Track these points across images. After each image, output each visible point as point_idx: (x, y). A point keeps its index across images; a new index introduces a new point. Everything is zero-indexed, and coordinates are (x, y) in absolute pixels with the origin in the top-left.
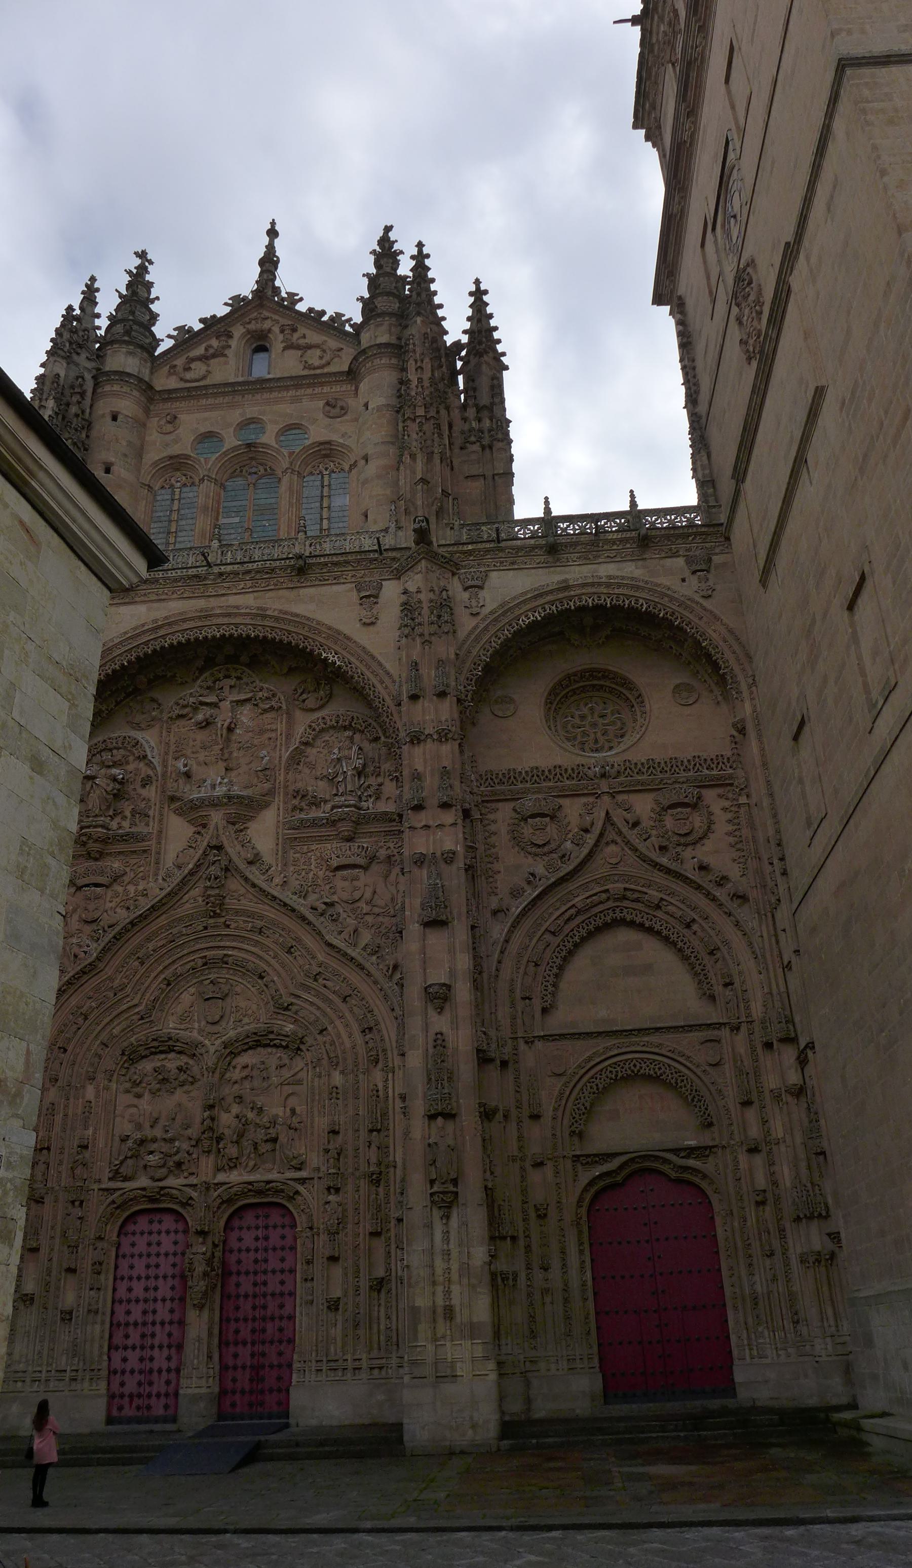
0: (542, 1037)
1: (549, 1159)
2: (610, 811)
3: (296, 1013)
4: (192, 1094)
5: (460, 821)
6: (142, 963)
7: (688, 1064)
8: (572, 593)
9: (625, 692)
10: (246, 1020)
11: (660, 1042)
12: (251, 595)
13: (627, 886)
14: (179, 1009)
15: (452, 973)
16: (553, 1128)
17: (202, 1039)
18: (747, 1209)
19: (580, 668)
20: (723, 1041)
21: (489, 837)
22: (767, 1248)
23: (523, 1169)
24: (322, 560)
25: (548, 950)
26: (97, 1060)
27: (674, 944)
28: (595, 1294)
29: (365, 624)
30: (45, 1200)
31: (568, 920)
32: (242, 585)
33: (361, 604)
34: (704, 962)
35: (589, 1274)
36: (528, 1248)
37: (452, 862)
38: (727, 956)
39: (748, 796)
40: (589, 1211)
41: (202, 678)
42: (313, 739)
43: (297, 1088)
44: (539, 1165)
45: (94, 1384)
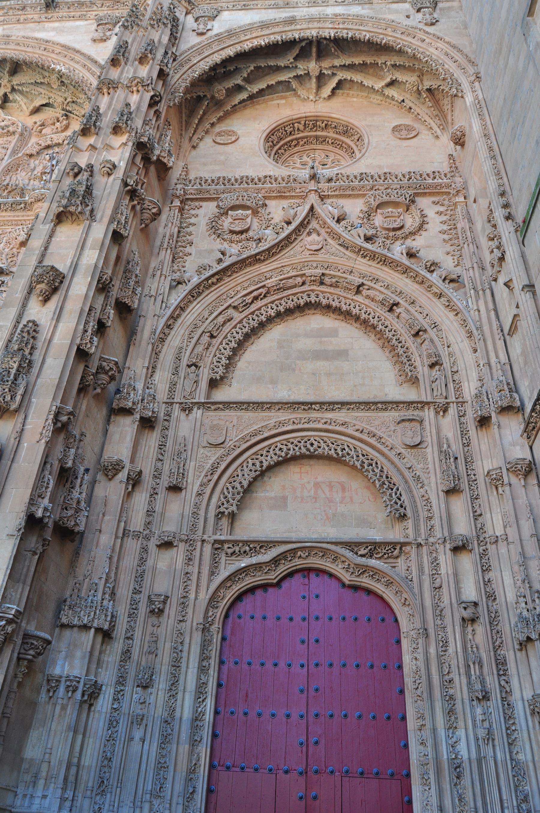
0: (203, 403)
1: (182, 541)
2: (315, 205)
5: (130, 144)
7: (379, 446)
8: (298, 27)
9: (347, 141)
11: (347, 420)
13: (327, 272)
15: (75, 267)
16: (197, 506)
18: (449, 629)
19: (304, 115)
20: (426, 423)
21: (187, 227)
22: (478, 687)
23: (145, 550)
25: (229, 324)
27: (374, 327)
28: (214, 736)
29: (95, 41)
31: (256, 298)
33: (97, 30)
34: (407, 345)
35: (209, 705)
36: (127, 654)
37: (109, 175)
38: (436, 339)
39: (465, 198)
40: (227, 616)
42: (38, 153)
44: (167, 545)
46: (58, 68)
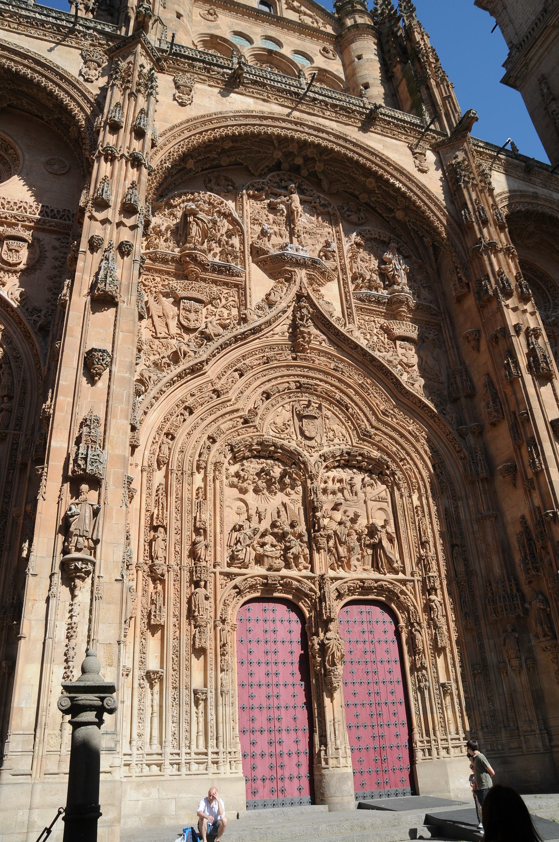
3: (380, 441)
4: (292, 497)
6: (241, 375)
8: (539, 202)
9: (540, 283)
10: (336, 441)
12: (334, 123)
14: (279, 421)
17: (301, 449)
24: (387, 118)
26: (205, 451)
30: (166, 577)
32: (329, 113)
41: (272, 174)
43: (384, 505)
45: (233, 767)
46: (398, 184)
